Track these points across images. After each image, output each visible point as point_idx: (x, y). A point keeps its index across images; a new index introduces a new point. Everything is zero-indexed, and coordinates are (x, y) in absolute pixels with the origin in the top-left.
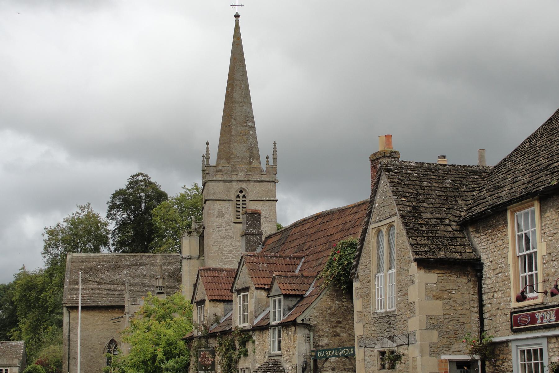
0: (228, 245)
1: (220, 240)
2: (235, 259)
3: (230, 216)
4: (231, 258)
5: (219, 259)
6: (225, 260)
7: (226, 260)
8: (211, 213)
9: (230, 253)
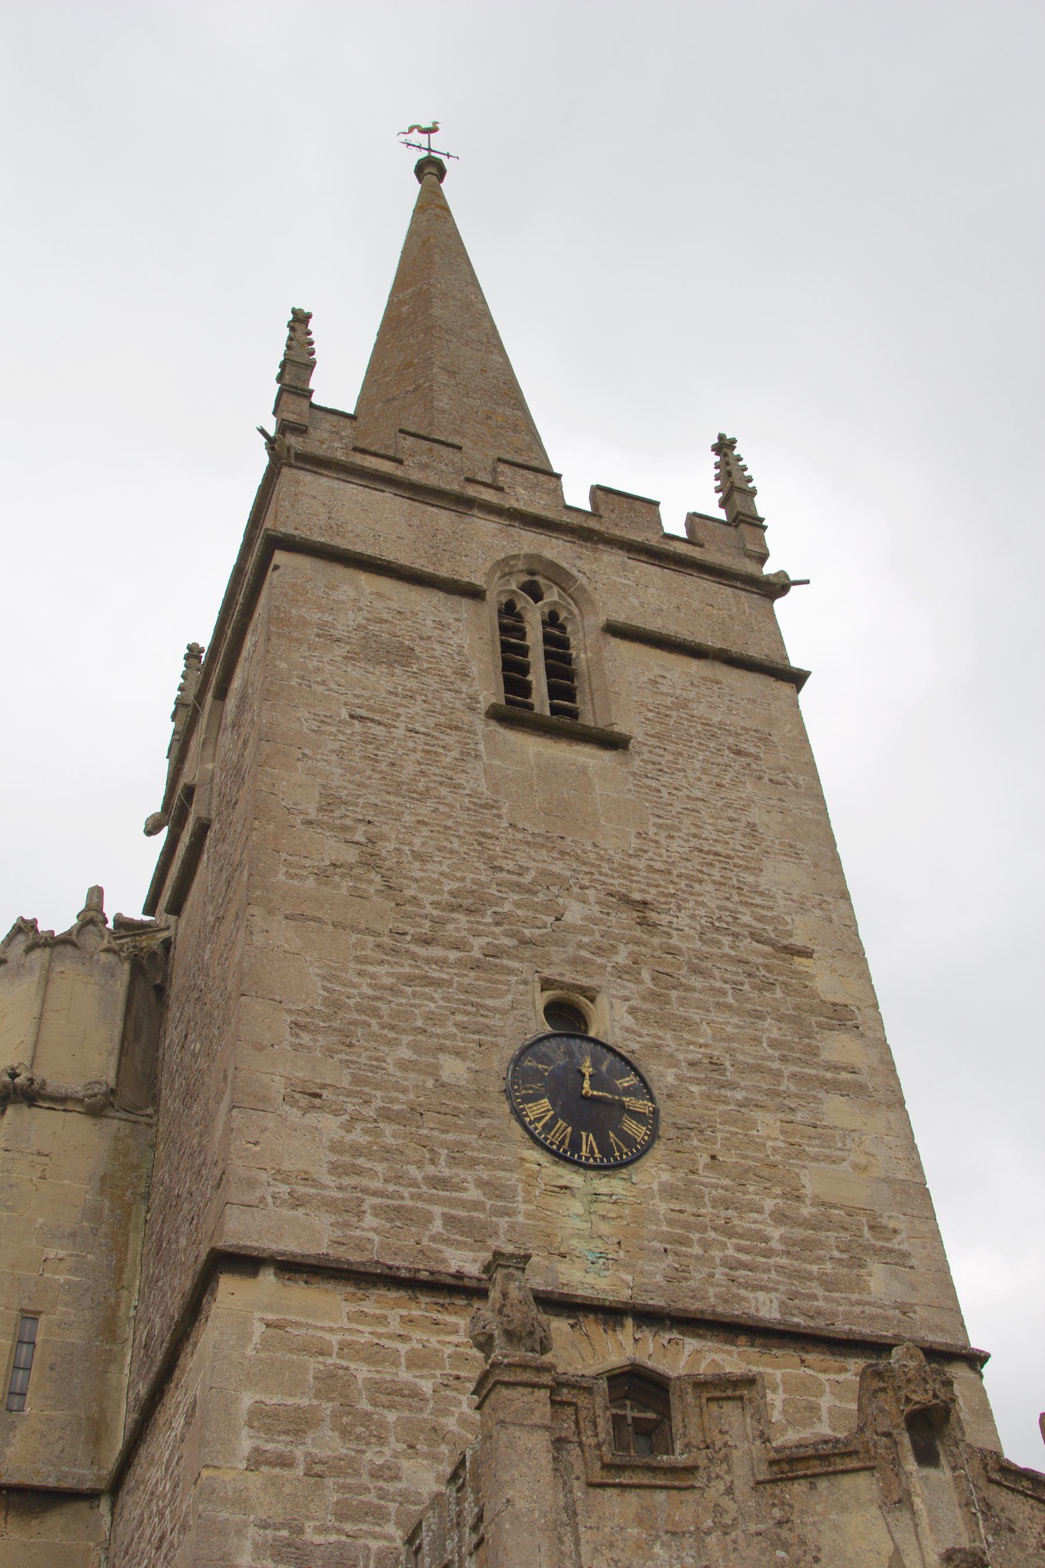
0: (452, 851)
1: (373, 799)
2: (516, 964)
3: (463, 674)
4: (478, 942)
5: (369, 931)
6: (422, 951)
7: (437, 952)
8: (304, 623)
9: (469, 911)
